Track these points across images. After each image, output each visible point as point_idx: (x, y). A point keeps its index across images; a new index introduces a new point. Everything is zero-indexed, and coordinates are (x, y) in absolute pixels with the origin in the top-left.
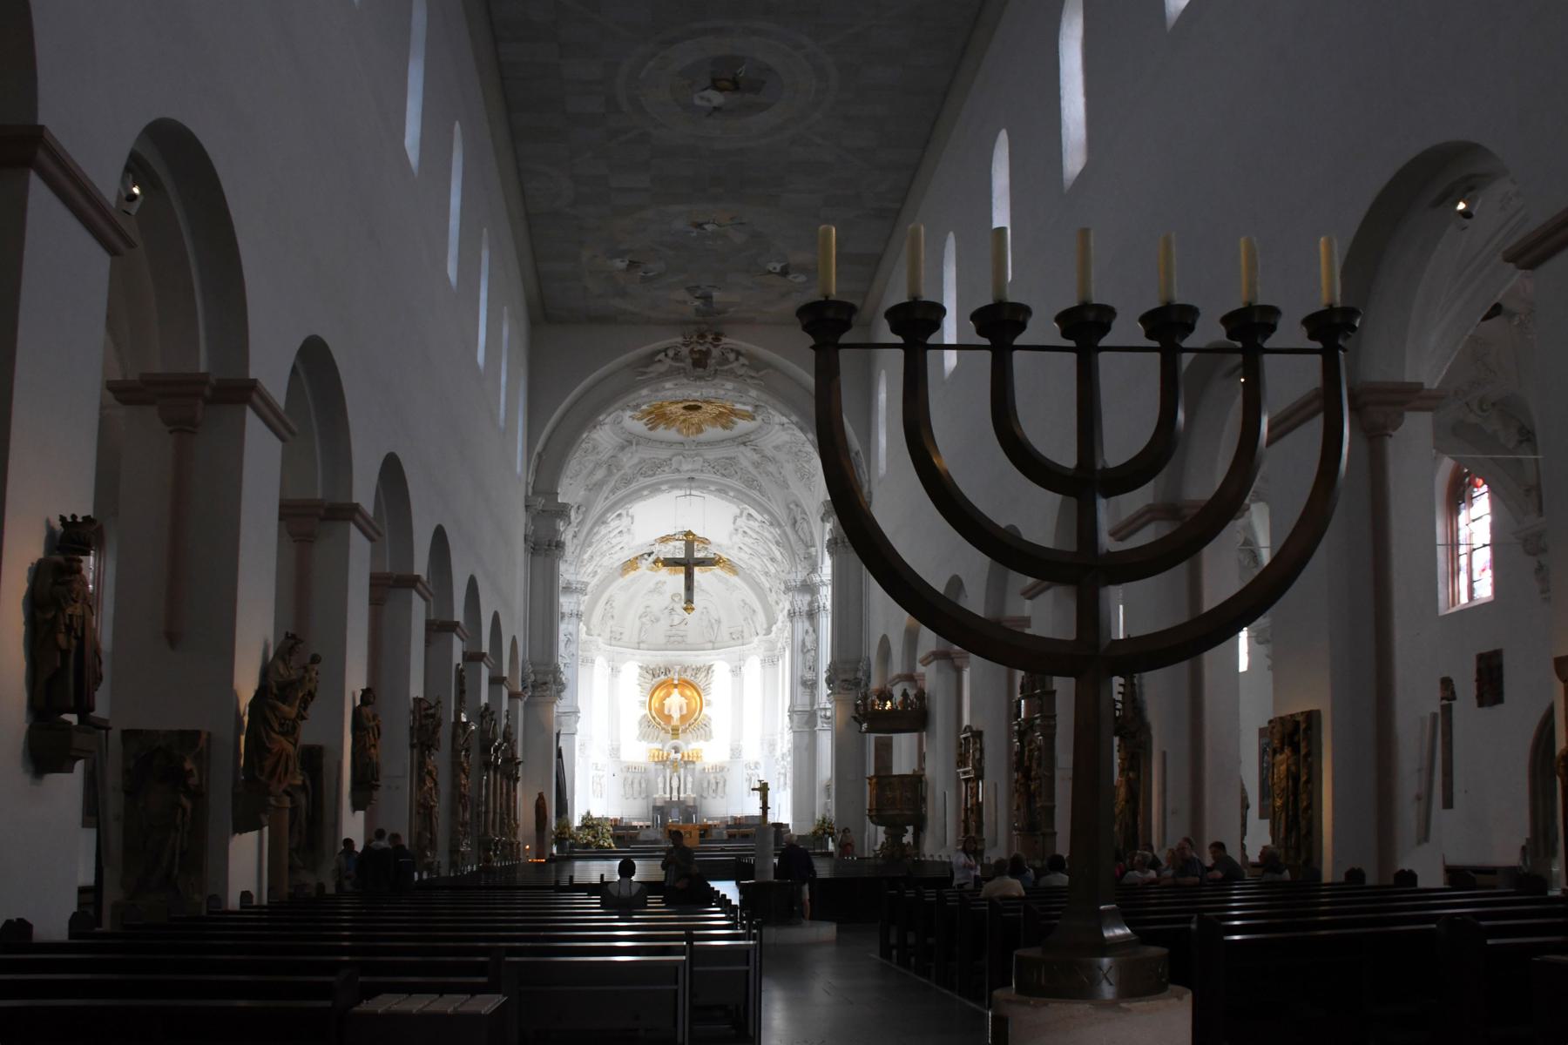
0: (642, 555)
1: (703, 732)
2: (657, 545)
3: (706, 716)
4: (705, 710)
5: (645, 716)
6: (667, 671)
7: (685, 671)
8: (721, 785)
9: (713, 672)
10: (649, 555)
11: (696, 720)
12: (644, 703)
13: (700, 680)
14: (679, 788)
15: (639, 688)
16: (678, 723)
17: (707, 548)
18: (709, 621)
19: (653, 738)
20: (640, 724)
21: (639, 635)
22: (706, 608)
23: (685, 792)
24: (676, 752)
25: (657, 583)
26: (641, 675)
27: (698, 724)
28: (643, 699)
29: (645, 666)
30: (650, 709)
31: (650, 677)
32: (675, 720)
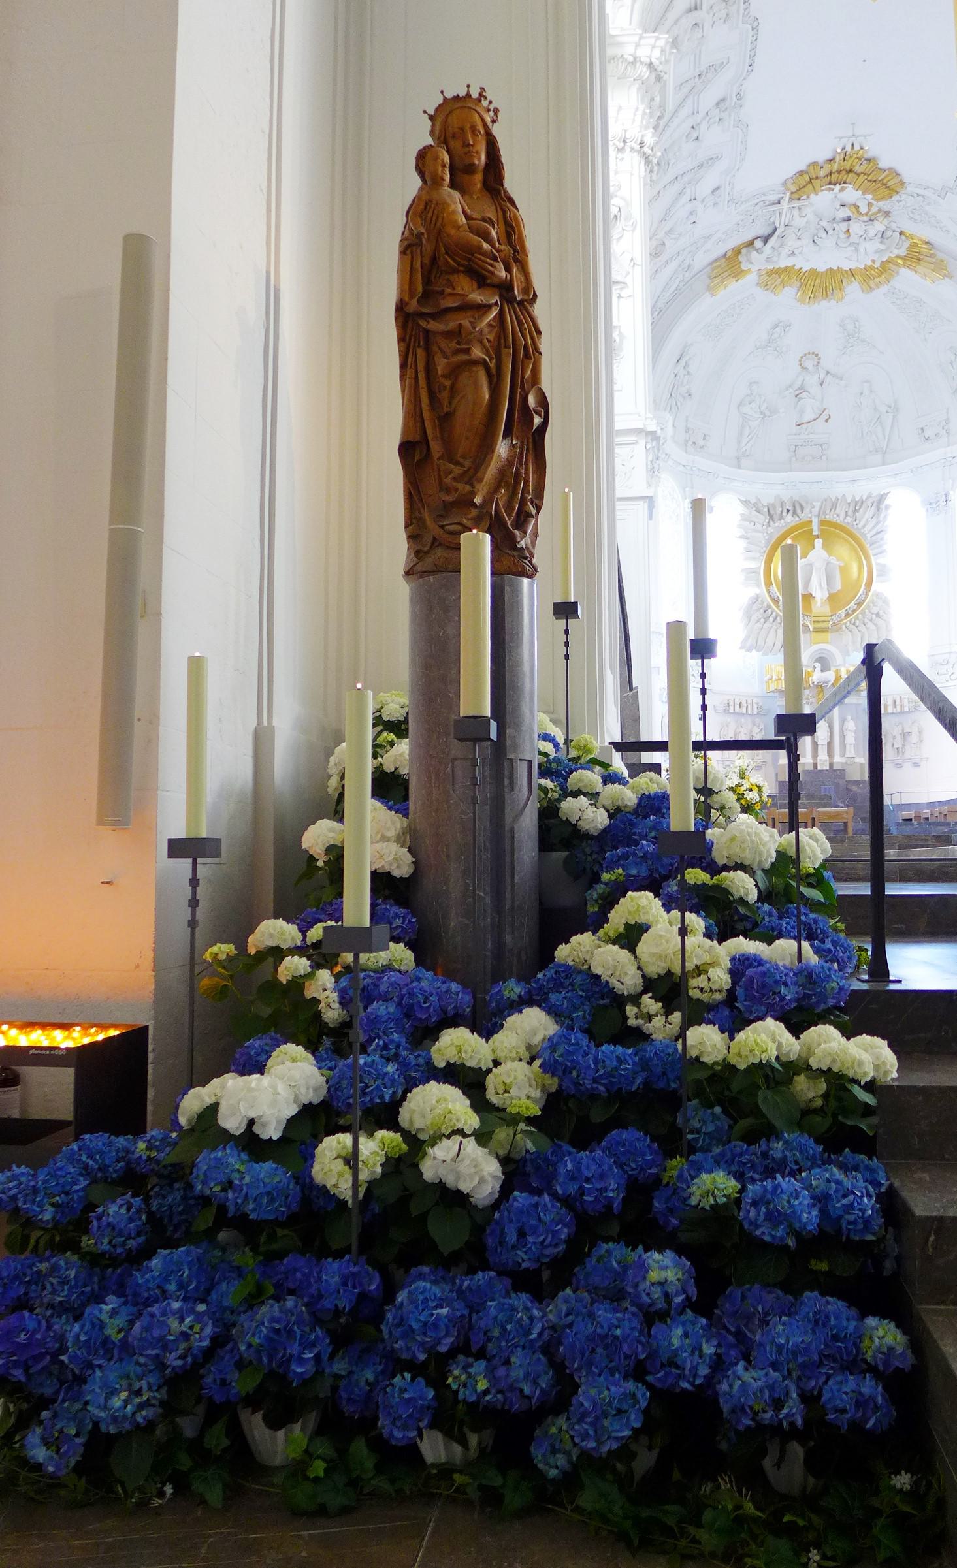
0: (751, 243)
1: (872, 627)
2: (785, 204)
3: (877, 595)
4: (876, 586)
5: (756, 599)
6: (796, 508)
7: (834, 506)
8: (914, 738)
9: (887, 507)
10: (766, 240)
11: (859, 604)
12: (755, 572)
13: (865, 523)
14: (830, 745)
15: (743, 544)
16: (827, 610)
17: (887, 214)
18: (875, 409)
19: (770, 642)
20: (748, 615)
21: (739, 442)
22: (867, 382)
23: (843, 755)
24: (822, 671)
25: (776, 326)
26: (745, 518)
27: (863, 613)
28: (753, 565)
29: (753, 501)
30: (768, 584)
31: (763, 518)
32: (819, 604)
